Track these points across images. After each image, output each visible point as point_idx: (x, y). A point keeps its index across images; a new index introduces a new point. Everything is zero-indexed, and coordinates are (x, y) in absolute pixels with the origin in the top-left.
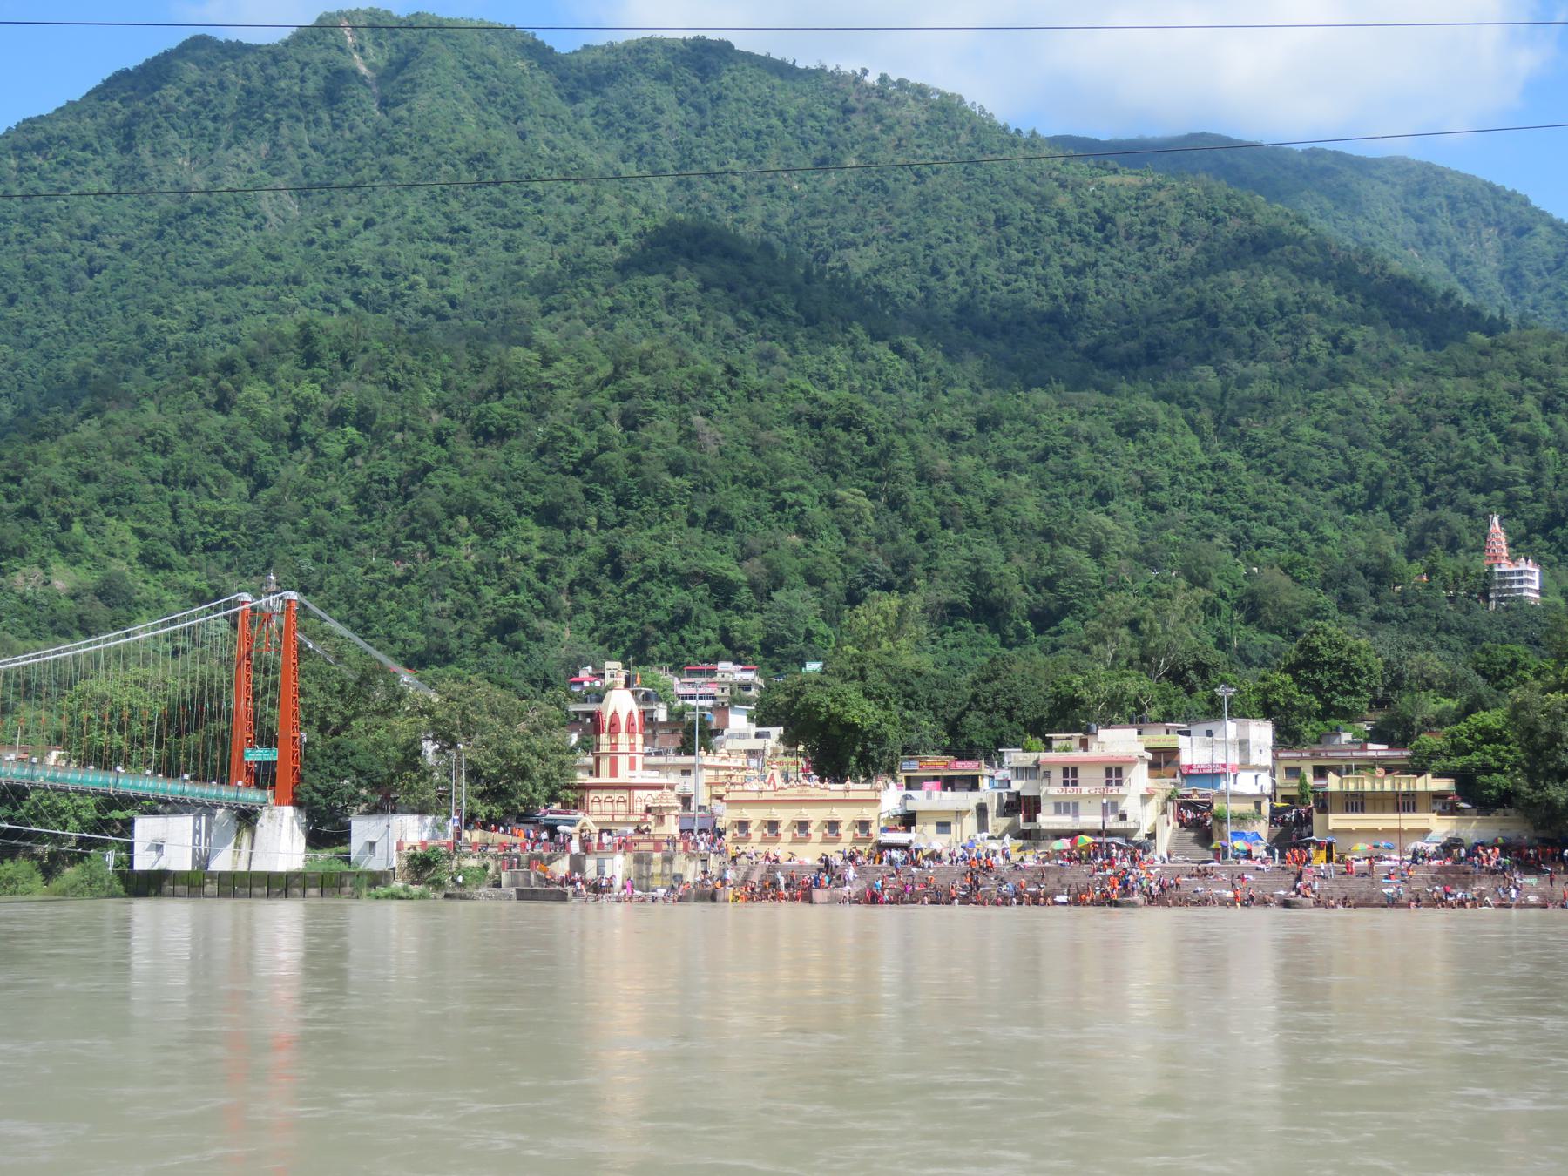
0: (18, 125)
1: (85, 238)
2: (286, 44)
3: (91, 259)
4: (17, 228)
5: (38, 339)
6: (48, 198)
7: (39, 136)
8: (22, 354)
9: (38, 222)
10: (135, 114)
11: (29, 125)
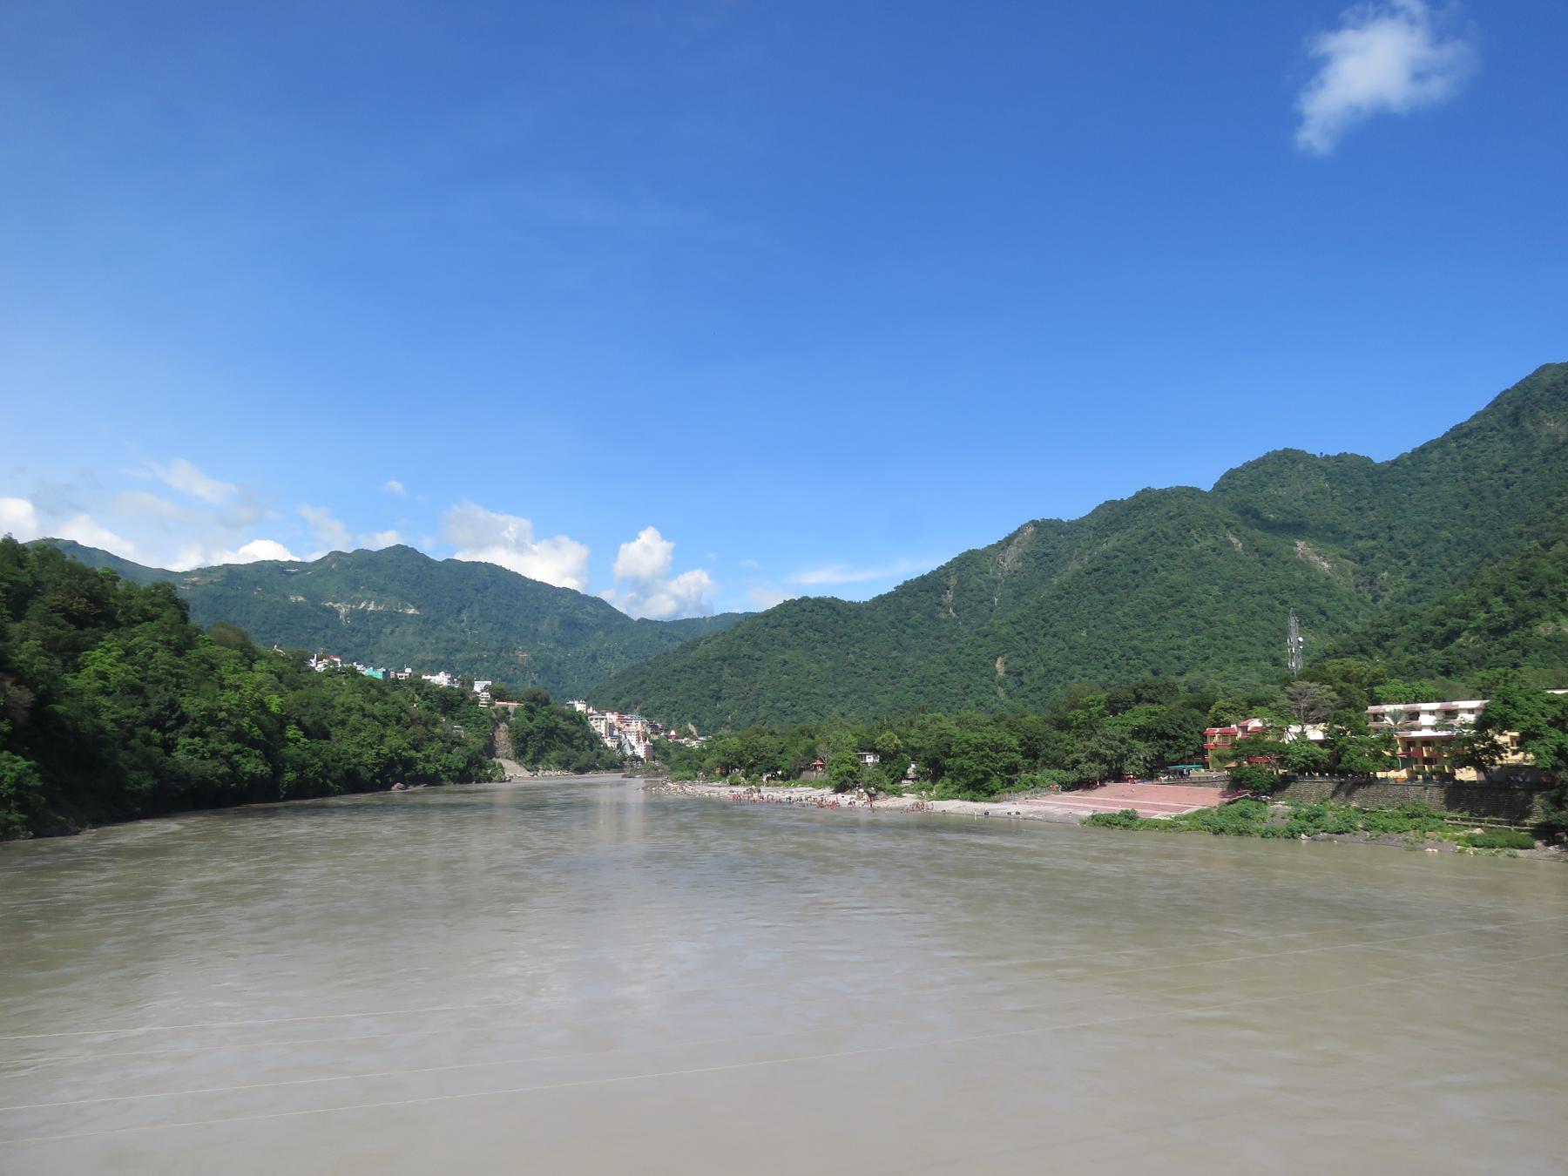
0: (1451, 430)
1: (1501, 471)
3: (1506, 480)
4: (1461, 474)
5: (1485, 522)
6: (1475, 458)
7: (1465, 430)
8: (1478, 530)
9: (1473, 468)
10: (1517, 408)
11: (1459, 427)
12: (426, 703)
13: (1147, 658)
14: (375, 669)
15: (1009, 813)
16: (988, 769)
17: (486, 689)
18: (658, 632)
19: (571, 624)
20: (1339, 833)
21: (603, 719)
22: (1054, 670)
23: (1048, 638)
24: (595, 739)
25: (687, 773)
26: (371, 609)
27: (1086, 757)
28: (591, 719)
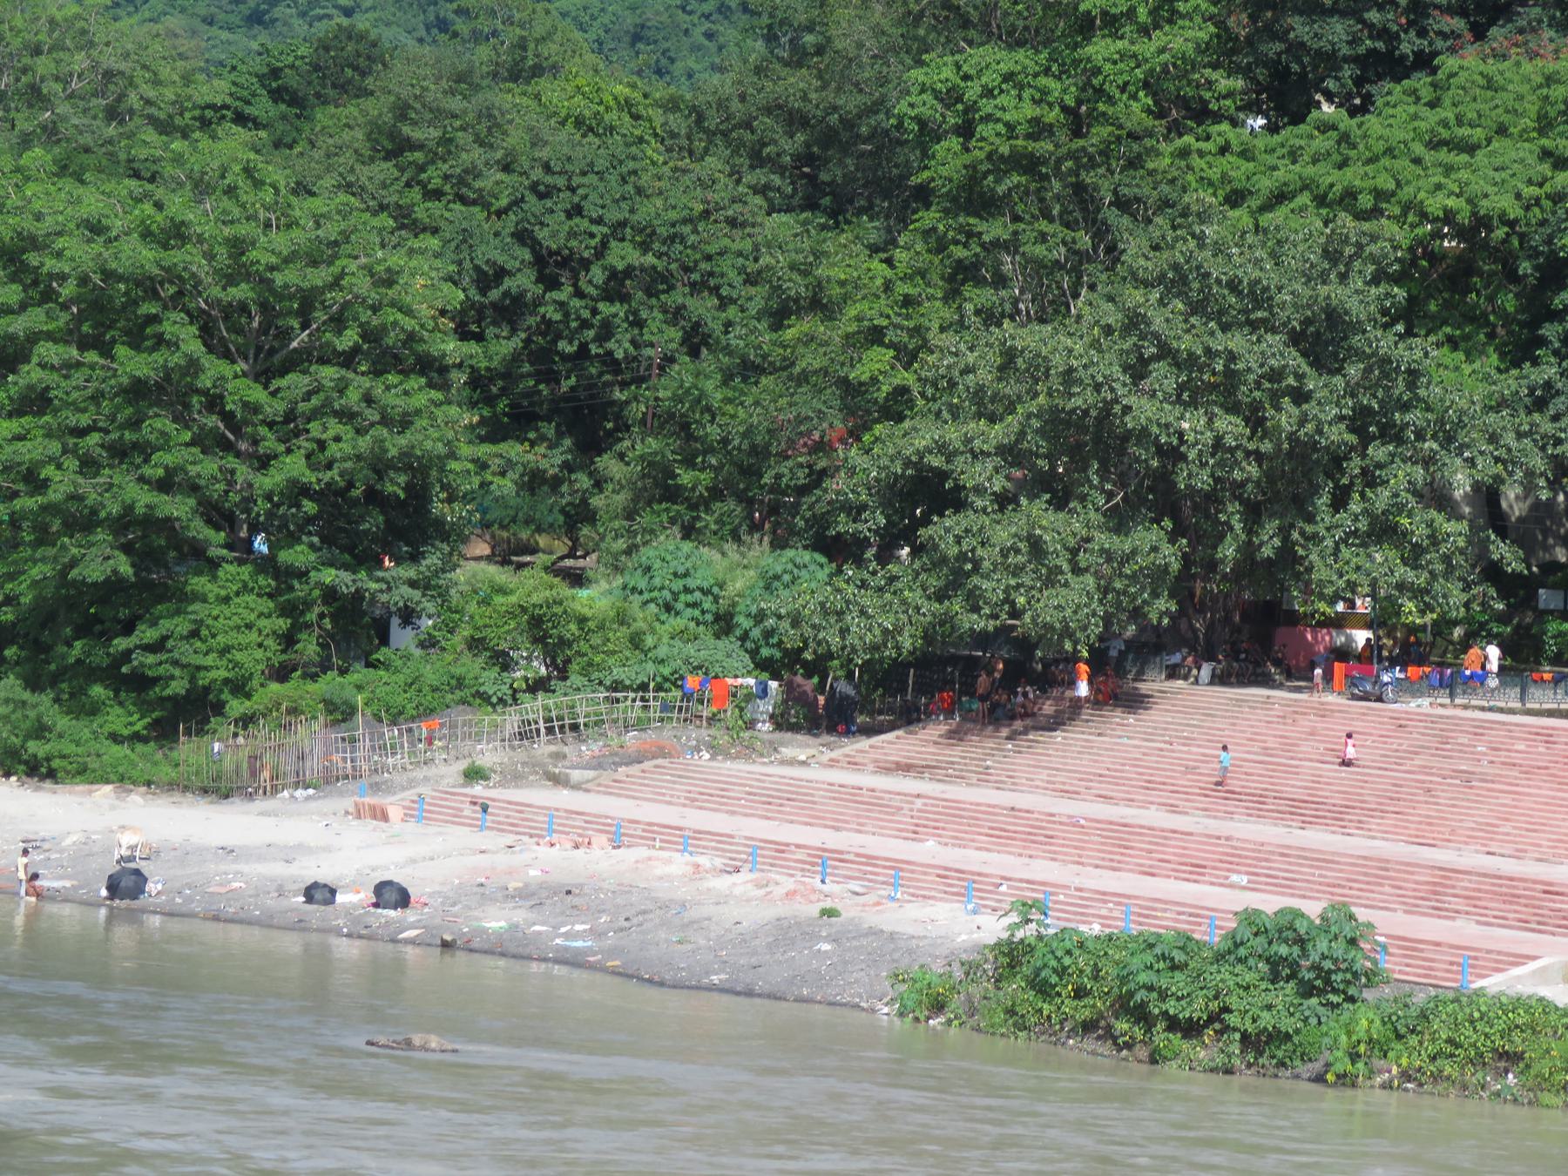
15: (321, 893)
16: (178, 507)
27: (1011, 453)
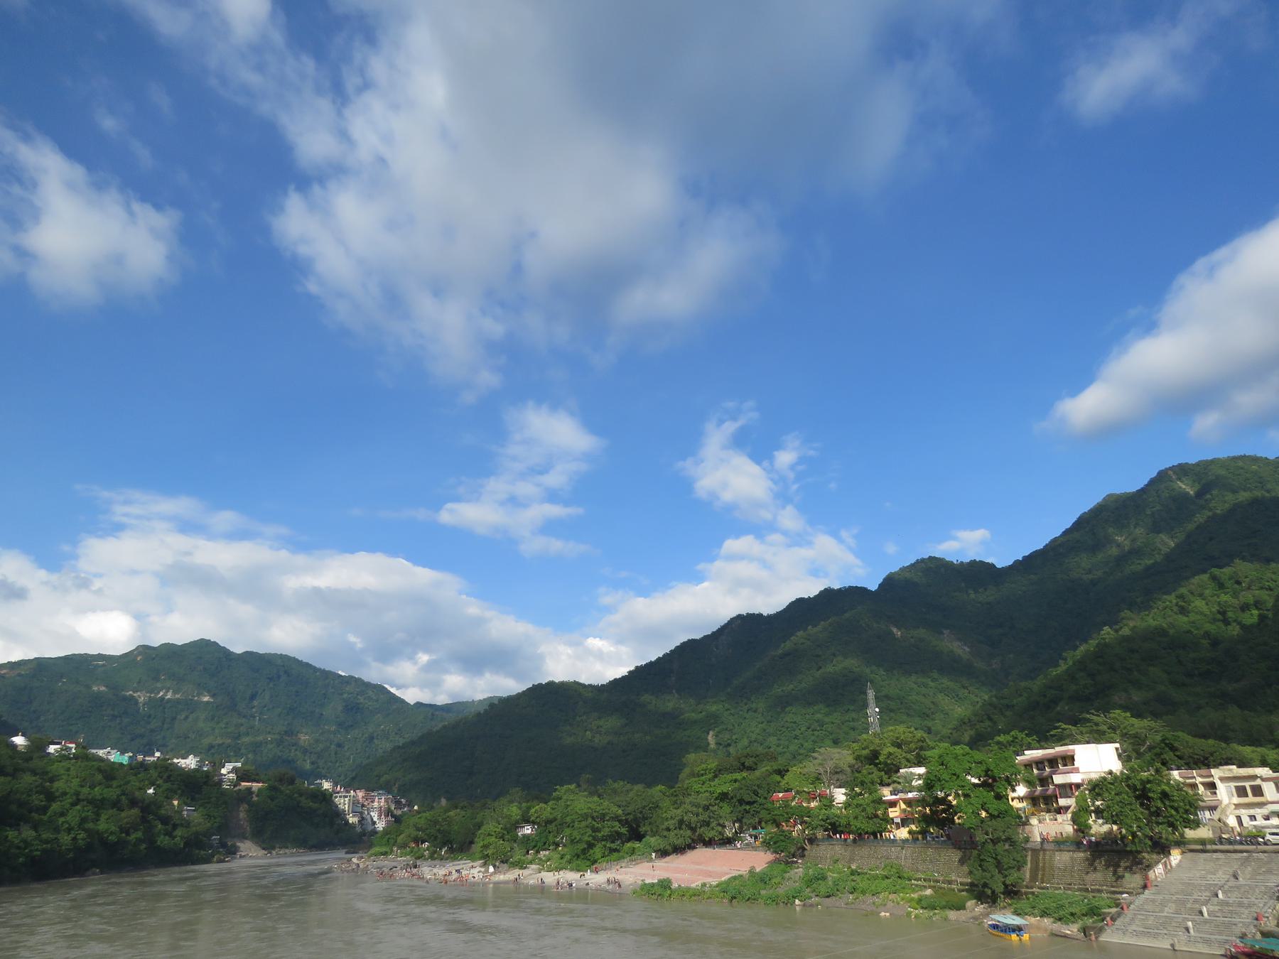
2: (1146, 485)
12: (168, 785)
13: (829, 730)
14: (123, 753)
17: (235, 770)
18: (430, 714)
19: (352, 708)
20: (828, 897)
21: (346, 797)
22: (755, 741)
23: (750, 713)
24: (336, 815)
25: (384, 849)
26: (169, 697)
28: (336, 797)
